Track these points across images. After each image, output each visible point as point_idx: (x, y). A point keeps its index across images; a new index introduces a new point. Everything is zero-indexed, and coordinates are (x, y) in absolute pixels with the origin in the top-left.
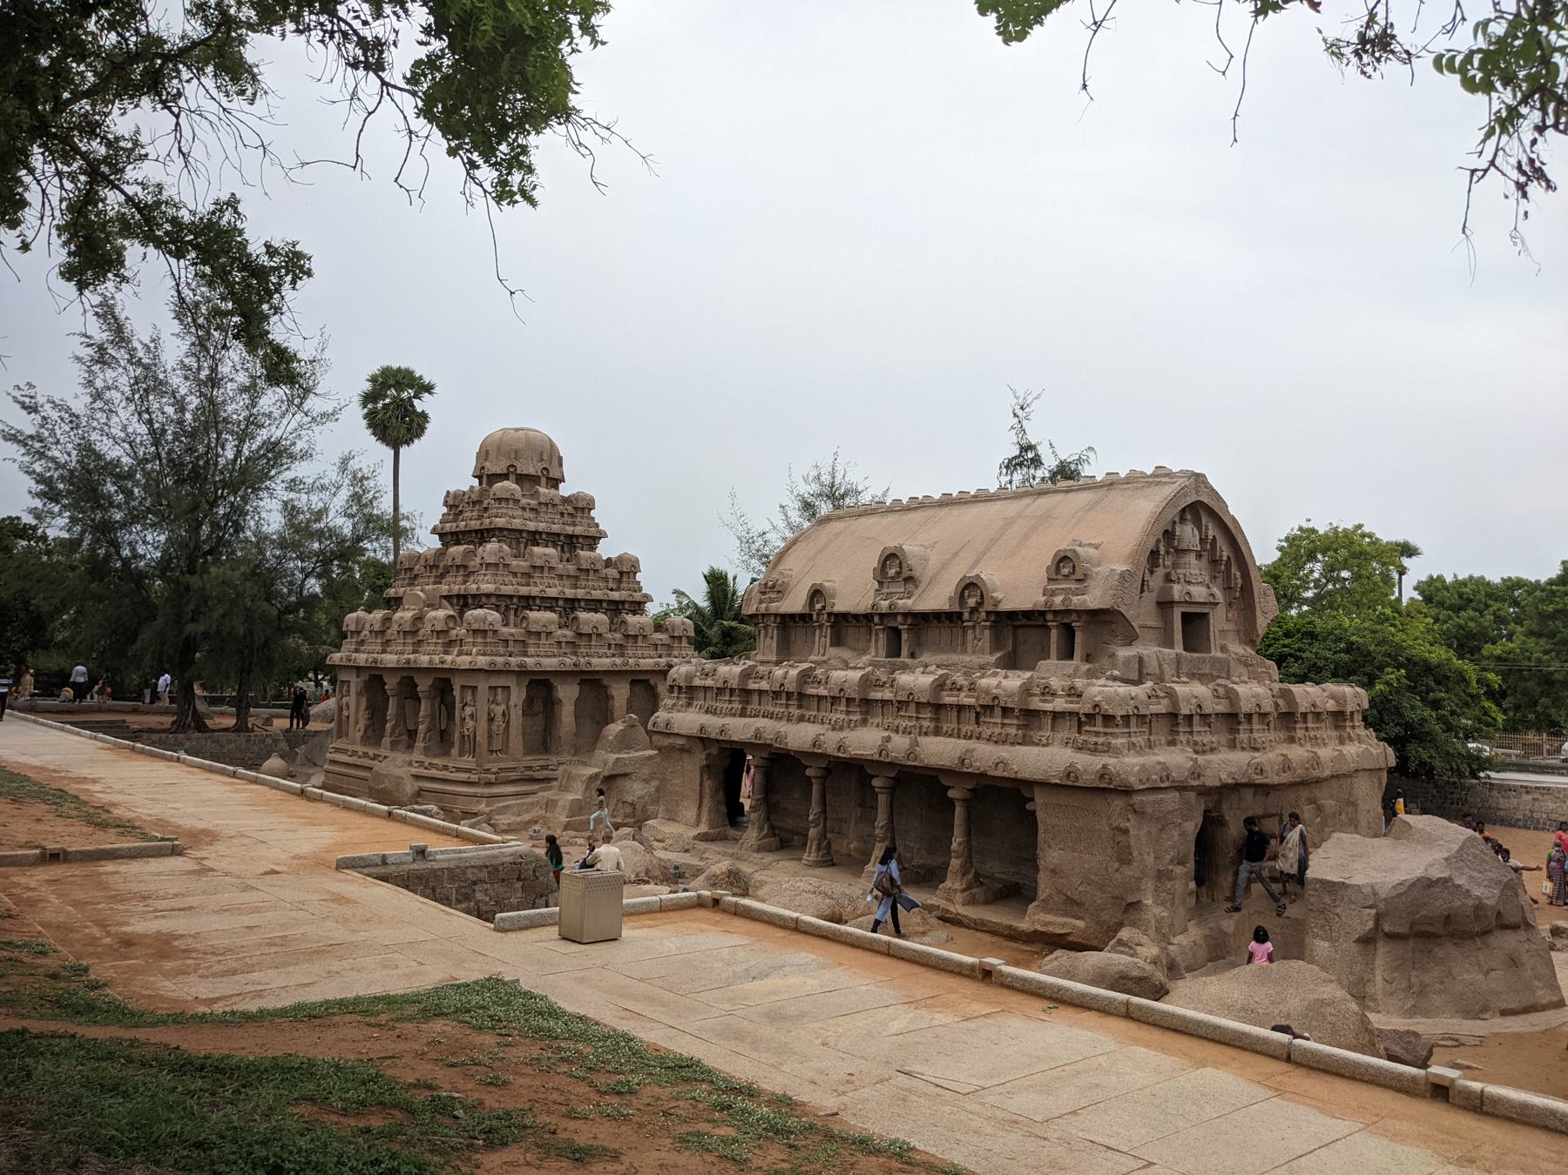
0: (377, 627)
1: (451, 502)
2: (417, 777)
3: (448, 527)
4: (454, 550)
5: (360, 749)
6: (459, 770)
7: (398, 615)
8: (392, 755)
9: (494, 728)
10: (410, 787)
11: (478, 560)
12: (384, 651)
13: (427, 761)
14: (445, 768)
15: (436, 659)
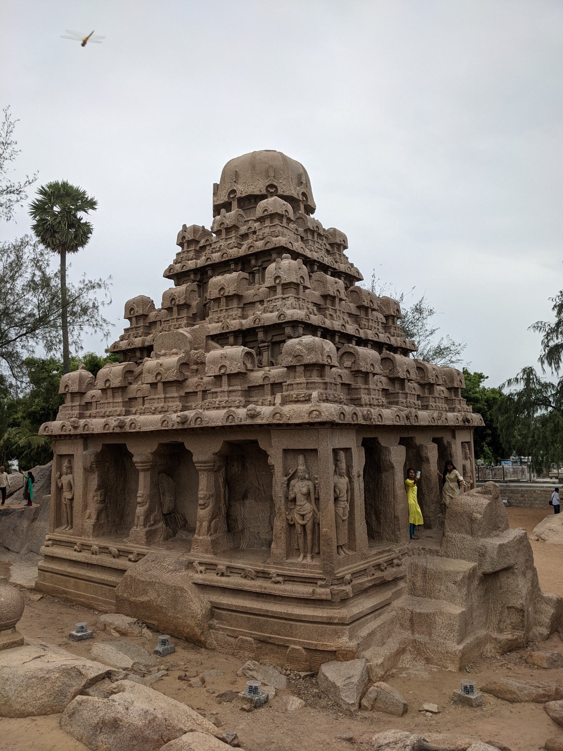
0: (116, 382)
1: (189, 237)
2: (203, 587)
3: (191, 264)
4: (217, 280)
5: (95, 543)
6: (290, 579)
7: (150, 363)
8: (153, 552)
9: (341, 511)
10: (198, 604)
11: (269, 282)
12: (128, 413)
13: (222, 563)
14: (264, 575)
15: (242, 412)
